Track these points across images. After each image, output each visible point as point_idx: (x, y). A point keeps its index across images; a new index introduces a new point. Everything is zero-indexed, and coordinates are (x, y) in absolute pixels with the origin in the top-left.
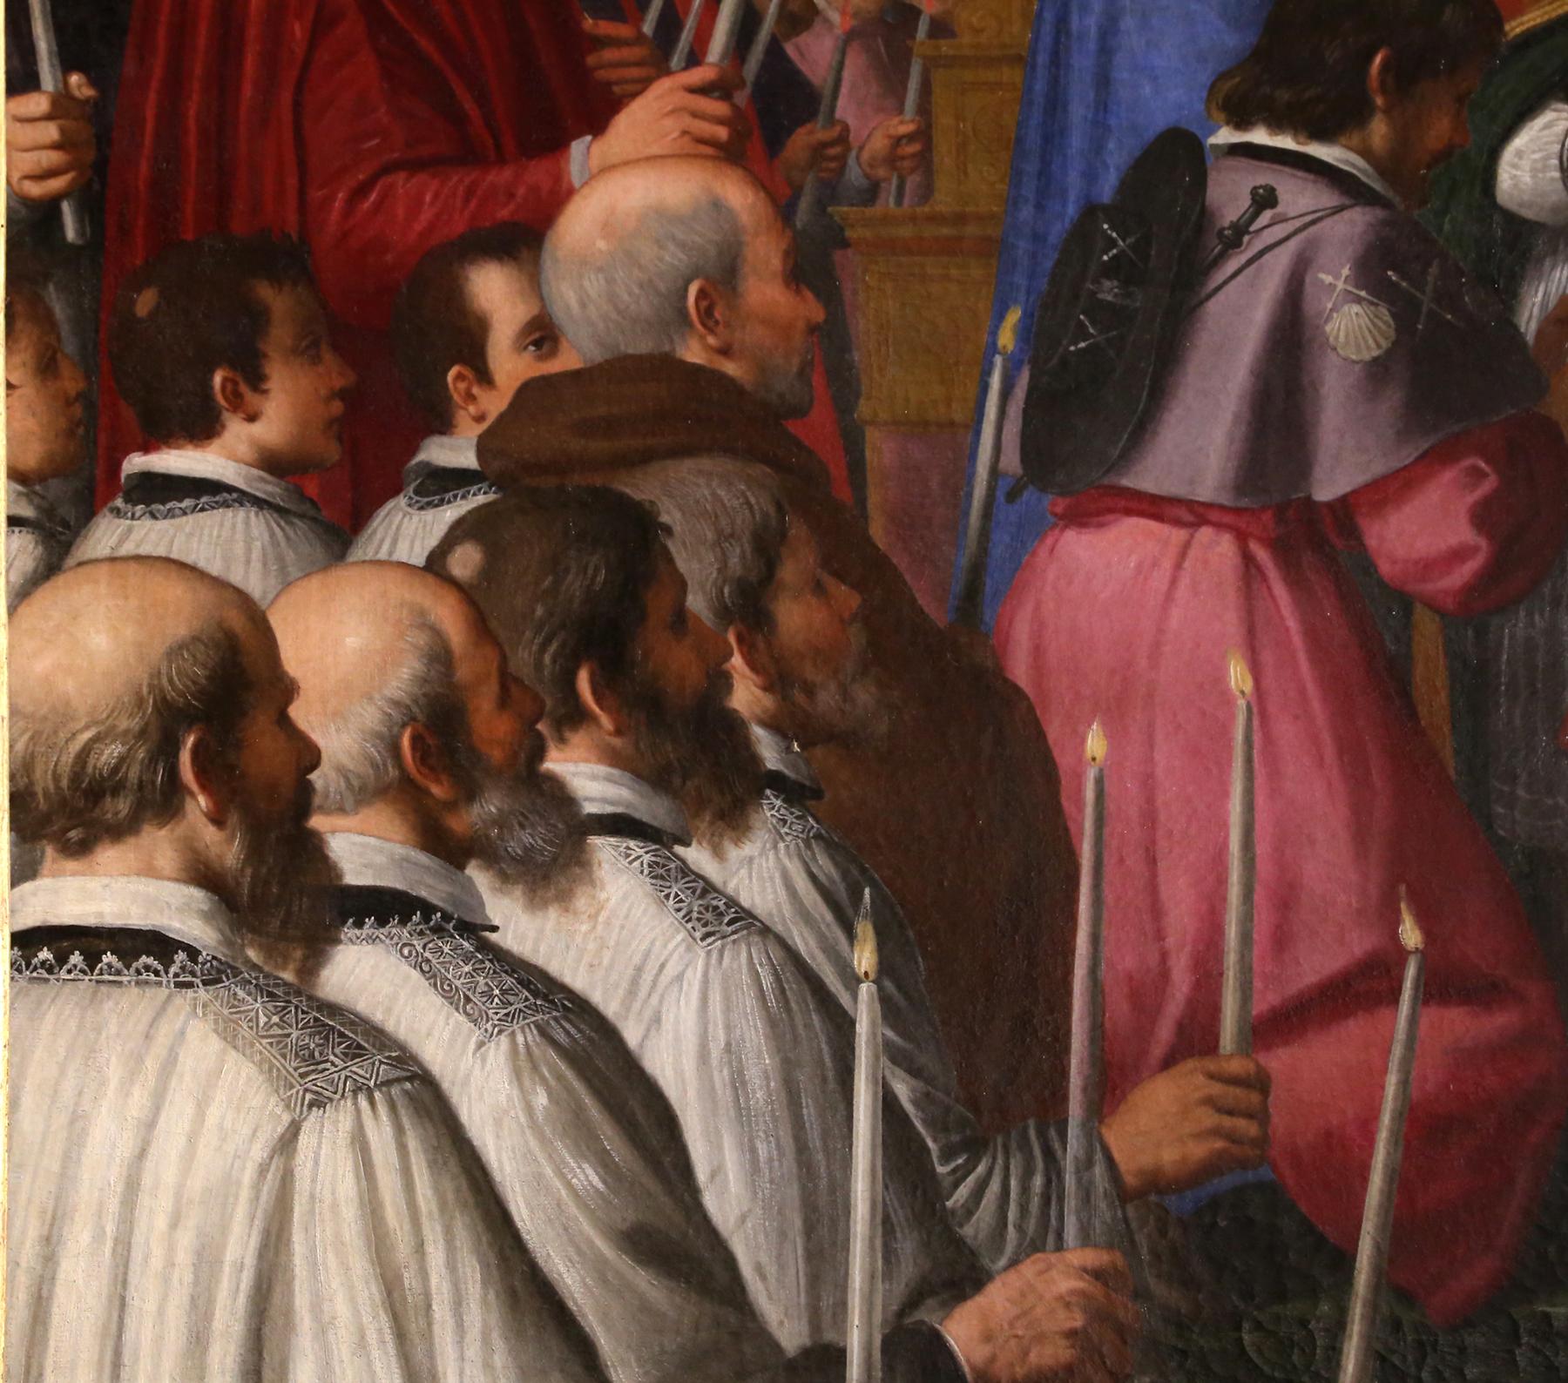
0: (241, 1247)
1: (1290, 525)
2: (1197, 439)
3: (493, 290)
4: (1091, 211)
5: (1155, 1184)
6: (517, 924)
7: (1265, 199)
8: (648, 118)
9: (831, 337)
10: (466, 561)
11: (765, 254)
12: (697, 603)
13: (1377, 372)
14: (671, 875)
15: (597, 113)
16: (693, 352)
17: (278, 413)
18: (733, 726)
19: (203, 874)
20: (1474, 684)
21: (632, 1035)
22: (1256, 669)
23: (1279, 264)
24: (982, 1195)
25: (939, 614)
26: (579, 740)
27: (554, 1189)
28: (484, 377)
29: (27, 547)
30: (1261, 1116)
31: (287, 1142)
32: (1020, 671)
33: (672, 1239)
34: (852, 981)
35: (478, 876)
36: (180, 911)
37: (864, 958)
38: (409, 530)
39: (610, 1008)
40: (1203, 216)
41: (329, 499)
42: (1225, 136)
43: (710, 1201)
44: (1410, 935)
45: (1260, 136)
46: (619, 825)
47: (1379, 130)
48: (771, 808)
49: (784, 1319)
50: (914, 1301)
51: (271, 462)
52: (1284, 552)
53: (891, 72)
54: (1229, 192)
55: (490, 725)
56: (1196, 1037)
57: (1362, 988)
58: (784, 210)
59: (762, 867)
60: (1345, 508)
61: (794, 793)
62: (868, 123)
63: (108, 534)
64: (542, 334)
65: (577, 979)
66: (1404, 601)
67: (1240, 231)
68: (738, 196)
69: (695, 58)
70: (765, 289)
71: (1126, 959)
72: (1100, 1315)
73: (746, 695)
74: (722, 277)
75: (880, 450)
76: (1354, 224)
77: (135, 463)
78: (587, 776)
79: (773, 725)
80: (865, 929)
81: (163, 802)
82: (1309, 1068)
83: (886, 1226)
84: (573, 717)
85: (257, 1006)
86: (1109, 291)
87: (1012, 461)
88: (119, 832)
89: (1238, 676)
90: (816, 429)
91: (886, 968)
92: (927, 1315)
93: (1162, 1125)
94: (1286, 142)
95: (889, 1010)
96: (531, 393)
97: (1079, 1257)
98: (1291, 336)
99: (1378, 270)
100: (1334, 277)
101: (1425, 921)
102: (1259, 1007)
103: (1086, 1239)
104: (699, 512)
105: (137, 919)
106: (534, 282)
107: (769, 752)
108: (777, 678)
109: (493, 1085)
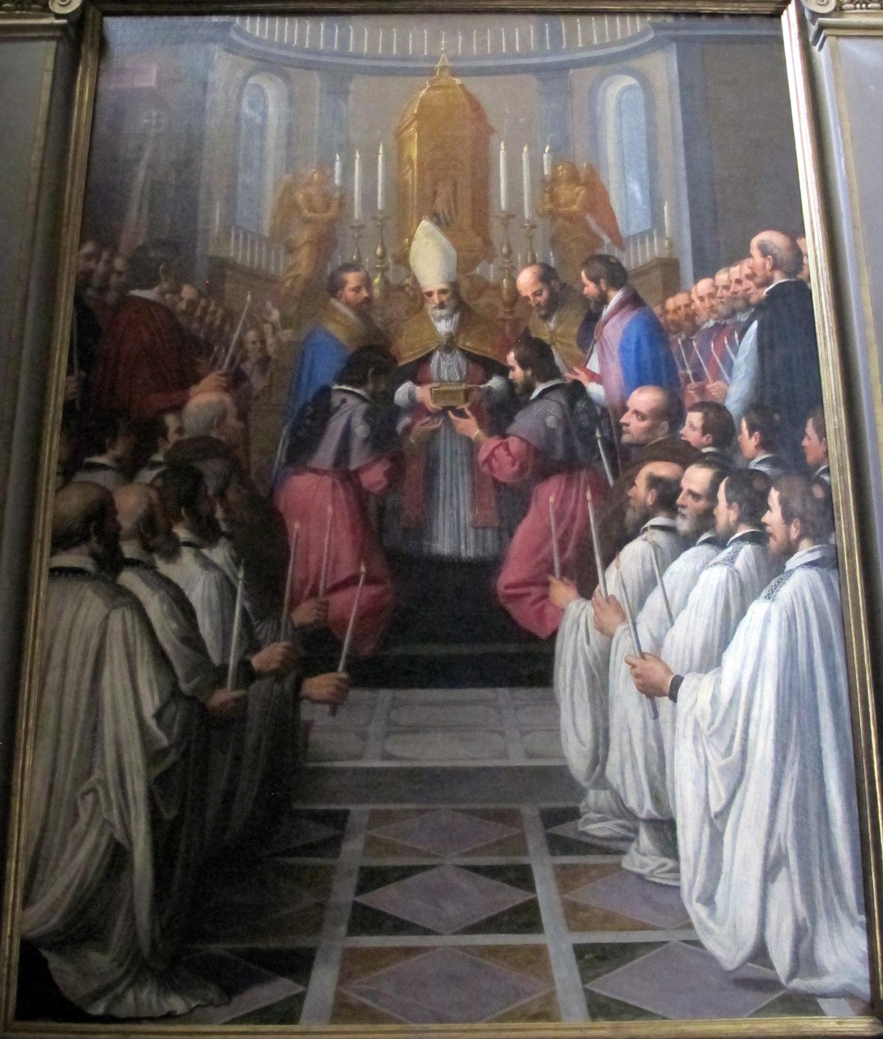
0: (94, 642)
1: (345, 474)
2: (325, 454)
3: (171, 421)
4: (306, 404)
5: (302, 627)
6: (163, 567)
7: (344, 401)
8: (210, 381)
9: (246, 431)
10: (159, 483)
11: (233, 411)
12: (210, 492)
13: (366, 441)
14: (199, 556)
15: (197, 380)
16: (214, 434)
17: (119, 449)
18: (216, 522)
19: (93, 555)
20: (382, 511)
21: (187, 593)
22: (334, 508)
23: (346, 416)
24: (263, 629)
25: (264, 495)
26: (181, 524)
27: (166, 627)
28: (166, 439)
29: (60, 478)
30: (326, 611)
31: (107, 617)
32: (281, 508)
33: (191, 638)
34: (238, 580)
35: (156, 557)
36: (88, 564)
37: (241, 575)
38: (148, 475)
39: (182, 585)
40: (329, 405)
41: (128, 471)
42: (336, 387)
43: (201, 631)
44: (363, 569)
45: (344, 387)
46: (188, 544)
47: (370, 386)
48: (223, 540)
49: (216, 659)
50: (246, 653)
51: (118, 460)
52: (342, 481)
53: (263, 371)
54: (336, 399)
55: (161, 521)
56: (314, 593)
57: (351, 581)
58: (237, 404)
59: (220, 554)
60: (357, 472)
61: (230, 537)
62: (257, 382)
63: (80, 477)
64: (180, 430)
65: (175, 580)
66: (368, 493)
67: (338, 409)
68: (227, 399)
69: (220, 368)
70: (232, 421)
71: (300, 575)
72: (286, 656)
73: (219, 514)
74: (222, 417)
75: (255, 457)
76: (362, 407)
77: (88, 460)
78: (182, 533)
79: (225, 520)
80: (242, 568)
81: (85, 538)
82: (338, 600)
83: (241, 636)
84: (178, 519)
85: (103, 585)
86: (308, 422)
87: (283, 460)
88: (76, 544)
89: (330, 509)
90: (239, 453)
91: (246, 577)
92: (248, 657)
93: (305, 614)
94: (350, 389)
95: (246, 587)
96: (178, 444)
97: (284, 643)
98: (347, 433)
99: (367, 417)
100: (357, 420)
101: (367, 565)
102: (329, 585)
103: (285, 639)
104: (212, 470)
105: (77, 565)
106: (180, 419)
107: (224, 527)
108: (227, 511)
109: (155, 606)
